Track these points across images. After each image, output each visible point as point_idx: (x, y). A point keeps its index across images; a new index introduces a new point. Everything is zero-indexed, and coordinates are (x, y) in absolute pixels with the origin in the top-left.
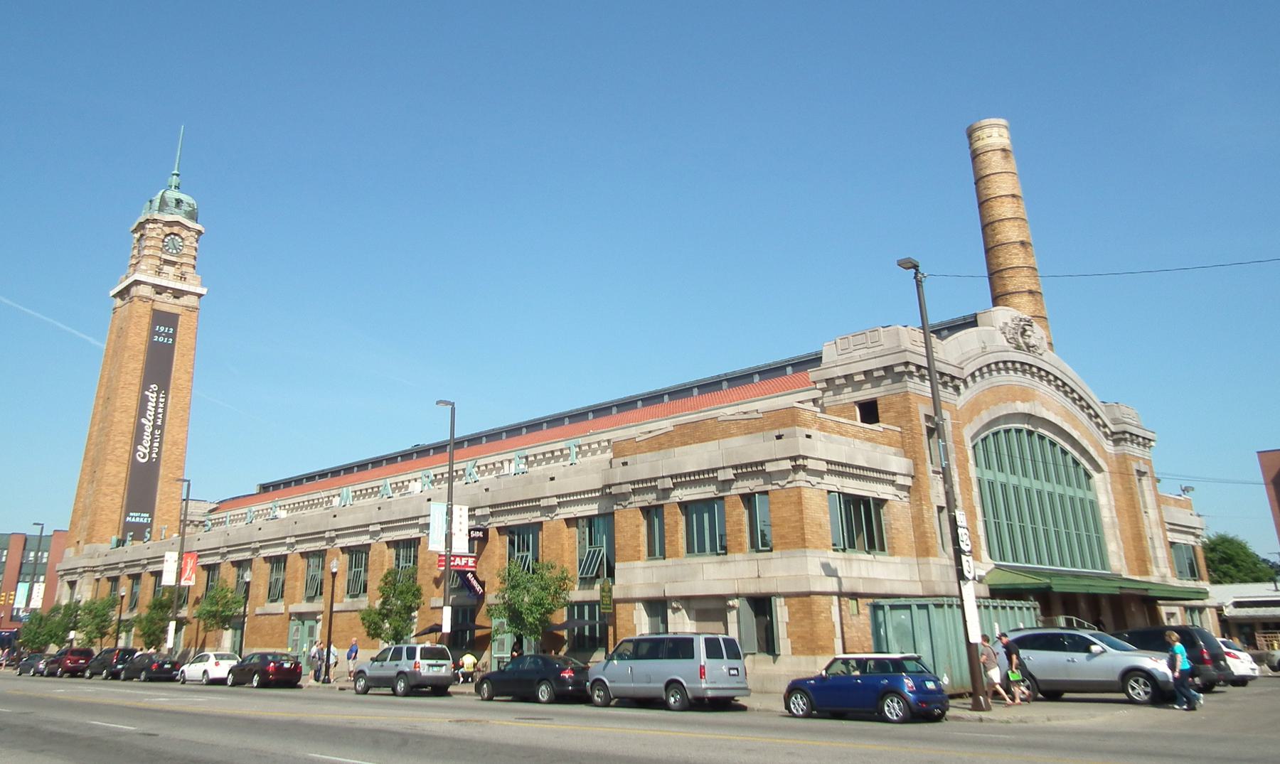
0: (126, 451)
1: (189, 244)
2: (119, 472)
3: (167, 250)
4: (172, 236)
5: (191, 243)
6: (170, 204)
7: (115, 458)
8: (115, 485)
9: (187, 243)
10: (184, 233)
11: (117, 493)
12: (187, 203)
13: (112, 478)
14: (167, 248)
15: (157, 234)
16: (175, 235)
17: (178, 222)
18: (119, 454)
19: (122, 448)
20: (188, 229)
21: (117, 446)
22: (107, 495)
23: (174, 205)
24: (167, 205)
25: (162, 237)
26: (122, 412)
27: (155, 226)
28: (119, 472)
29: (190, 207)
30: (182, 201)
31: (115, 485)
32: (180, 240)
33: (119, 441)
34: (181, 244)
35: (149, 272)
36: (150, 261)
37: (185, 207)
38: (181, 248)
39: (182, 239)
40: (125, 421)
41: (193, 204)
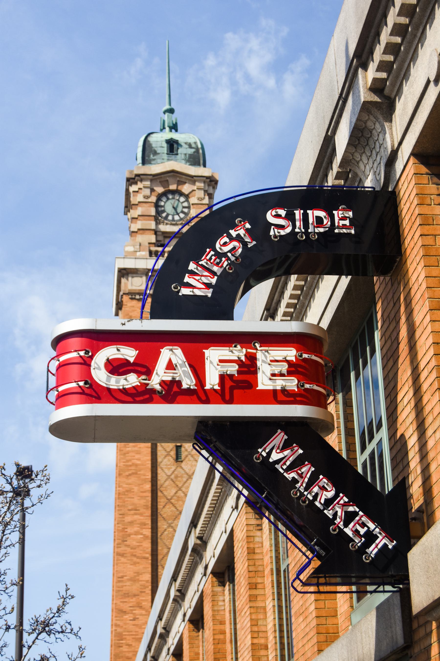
0: (145, 537)
1: (196, 201)
2: (138, 574)
3: (166, 218)
4: (170, 197)
5: (200, 199)
6: (159, 150)
7: (129, 550)
8: (135, 595)
9: (193, 200)
10: (186, 188)
11: (141, 607)
12: (186, 143)
13: (128, 583)
14: (164, 215)
15: (146, 197)
16: (173, 192)
17: (173, 171)
18: (135, 543)
19: (137, 533)
20: (192, 179)
21: (130, 530)
22: (125, 612)
23: (165, 150)
24: (155, 153)
25: (153, 199)
26: (130, 475)
27: (140, 185)
28: (138, 574)
29: (190, 146)
30: (177, 142)
31: (135, 595)
32: (182, 199)
33: (131, 523)
34: (186, 204)
35: (138, 254)
36: (140, 238)
37: (183, 151)
38: (186, 210)
39: (187, 197)
40: (136, 489)
41: (195, 143)
